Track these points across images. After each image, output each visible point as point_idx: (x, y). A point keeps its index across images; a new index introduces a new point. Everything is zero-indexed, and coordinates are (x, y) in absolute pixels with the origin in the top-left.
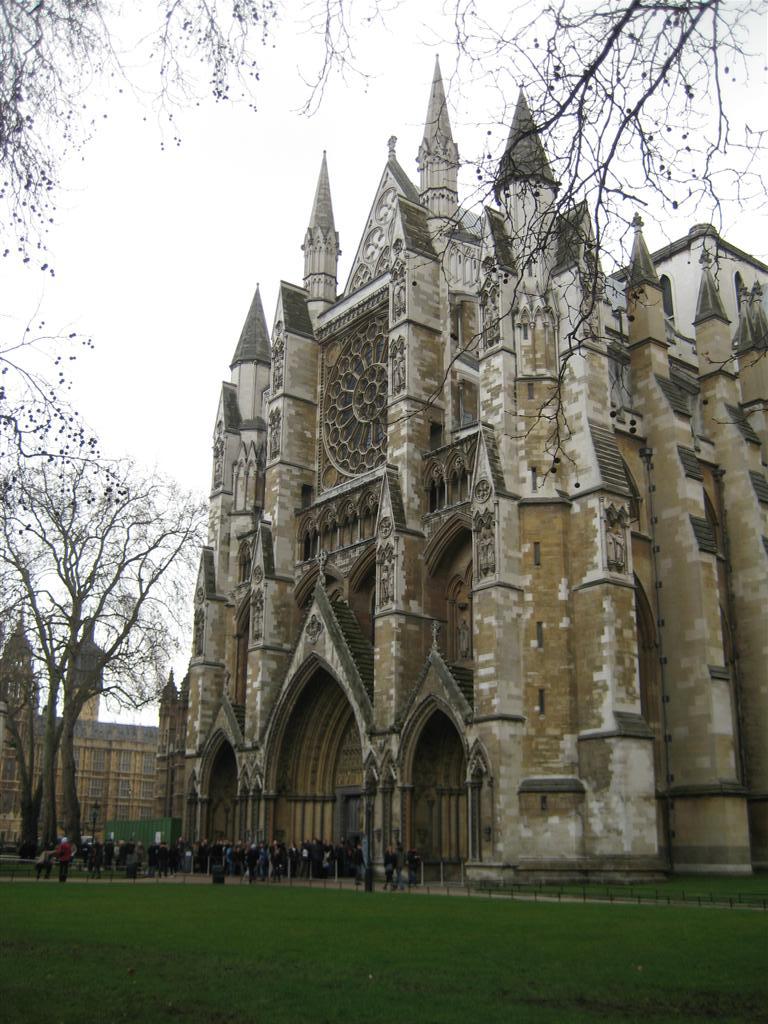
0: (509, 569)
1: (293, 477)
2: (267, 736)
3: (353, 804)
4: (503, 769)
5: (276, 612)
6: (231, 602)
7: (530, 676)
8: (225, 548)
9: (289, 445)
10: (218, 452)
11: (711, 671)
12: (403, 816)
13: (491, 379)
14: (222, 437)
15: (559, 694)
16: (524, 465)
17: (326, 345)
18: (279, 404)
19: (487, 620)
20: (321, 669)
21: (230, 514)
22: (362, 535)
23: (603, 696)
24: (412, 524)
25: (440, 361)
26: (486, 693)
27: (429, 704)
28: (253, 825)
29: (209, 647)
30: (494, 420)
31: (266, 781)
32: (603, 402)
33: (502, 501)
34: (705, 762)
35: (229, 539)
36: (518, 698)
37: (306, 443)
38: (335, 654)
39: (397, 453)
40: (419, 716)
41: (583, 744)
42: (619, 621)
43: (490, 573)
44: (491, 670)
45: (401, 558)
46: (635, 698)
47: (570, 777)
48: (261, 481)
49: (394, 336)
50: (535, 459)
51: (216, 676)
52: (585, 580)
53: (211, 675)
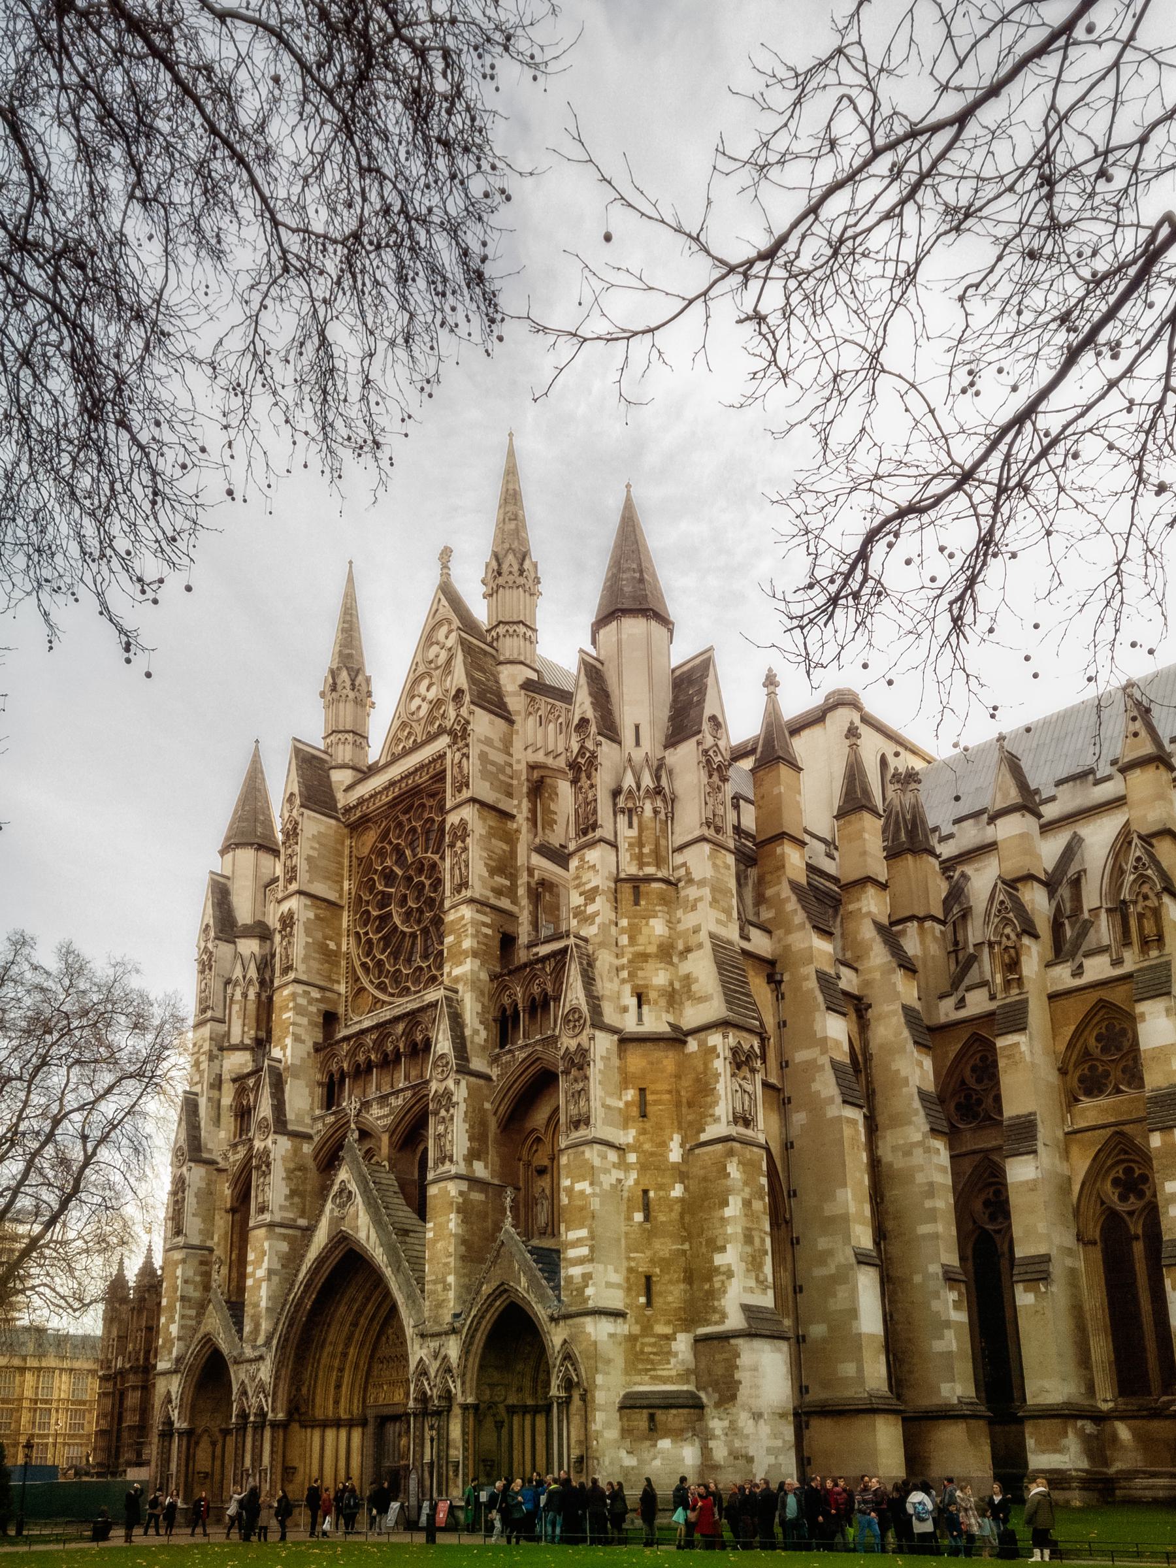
0: (608, 1122)
1: (311, 1001)
2: (275, 1342)
3: (392, 1429)
4: (599, 1379)
6: (222, 1164)
7: (634, 1259)
8: (215, 1094)
9: (306, 959)
10: (206, 965)
11: (856, 1254)
12: (465, 1441)
15: (670, 1282)
16: (627, 989)
17: (357, 825)
19: (578, 1187)
20: (351, 1251)
21: (221, 1049)
22: (407, 1078)
23: (727, 1283)
24: (478, 1063)
25: (513, 854)
26: (578, 1280)
27: (500, 1295)
28: (253, 1460)
29: (193, 1225)
30: (589, 931)
32: (728, 912)
33: (598, 1033)
34: (848, 1369)
35: (221, 1081)
36: (618, 1286)
37: (330, 957)
39: (457, 971)
40: (487, 1311)
41: (700, 1345)
42: (747, 1190)
43: (583, 1126)
44: (584, 1251)
45: (463, 1107)
46: (767, 1287)
47: (685, 1388)
48: (265, 1010)
49: (453, 819)
50: (641, 983)
51: (202, 1263)
52: (704, 1137)
53: (193, 1263)
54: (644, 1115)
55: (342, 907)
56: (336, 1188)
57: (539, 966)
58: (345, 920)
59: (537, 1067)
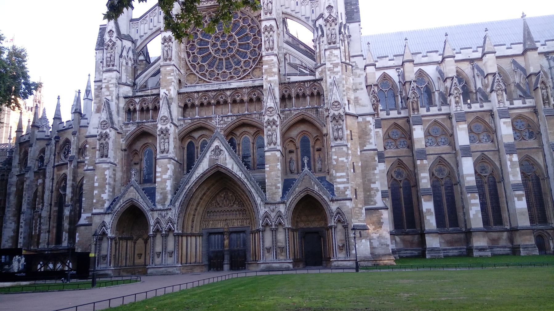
2: (177, 204)
5: (174, 141)
6: (120, 131)
8: (117, 101)
13: (333, 58)
14: (114, 39)
19: (340, 159)
21: (119, 84)
30: (337, 77)
31: (177, 226)
37: (180, 57)
39: (269, 79)
41: (367, 211)
43: (339, 139)
44: (345, 180)
51: (114, 170)
52: (365, 148)
53: (111, 170)
54: (352, 139)
56: (212, 148)
57: (302, 83)
59: (301, 117)
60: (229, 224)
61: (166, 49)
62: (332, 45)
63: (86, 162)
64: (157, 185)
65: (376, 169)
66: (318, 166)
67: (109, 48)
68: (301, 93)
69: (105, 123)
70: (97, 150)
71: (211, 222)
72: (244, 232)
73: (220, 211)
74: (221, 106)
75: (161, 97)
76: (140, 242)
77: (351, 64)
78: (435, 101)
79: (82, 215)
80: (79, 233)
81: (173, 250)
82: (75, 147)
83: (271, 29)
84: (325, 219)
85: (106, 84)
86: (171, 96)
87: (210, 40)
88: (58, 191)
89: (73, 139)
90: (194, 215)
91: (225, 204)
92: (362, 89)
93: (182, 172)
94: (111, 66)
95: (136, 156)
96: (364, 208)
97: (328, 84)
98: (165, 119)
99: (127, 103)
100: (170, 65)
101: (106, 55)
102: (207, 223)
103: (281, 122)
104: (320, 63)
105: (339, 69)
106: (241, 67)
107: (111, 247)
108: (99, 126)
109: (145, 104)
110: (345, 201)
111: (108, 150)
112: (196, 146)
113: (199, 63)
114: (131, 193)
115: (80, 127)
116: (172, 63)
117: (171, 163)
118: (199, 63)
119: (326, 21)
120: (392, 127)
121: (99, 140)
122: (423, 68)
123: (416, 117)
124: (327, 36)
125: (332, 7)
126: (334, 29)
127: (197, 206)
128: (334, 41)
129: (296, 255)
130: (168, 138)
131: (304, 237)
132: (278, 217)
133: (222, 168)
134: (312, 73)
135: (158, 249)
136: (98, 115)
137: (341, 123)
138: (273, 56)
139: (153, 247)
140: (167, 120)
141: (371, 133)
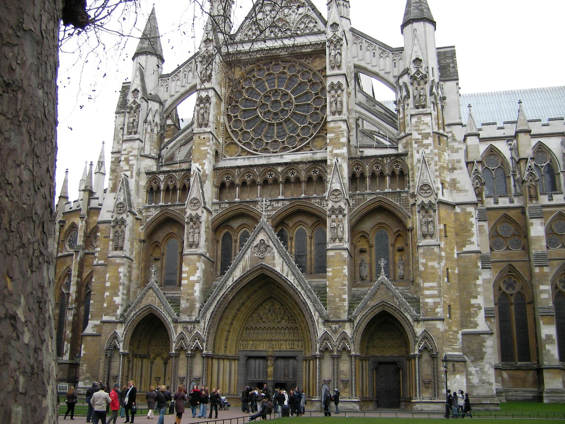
2: (208, 315)
5: (206, 232)
6: (139, 216)
13: (421, 128)
14: (138, 101)
16: (439, 180)
18: (211, 94)
19: (430, 264)
21: (141, 156)
31: (207, 345)
38: (286, 268)
39: (336, 151)
41: (464, 336)
43: (428, 237)
44: (436, 292)
51: (130, 267)
52: (465, 249)
55: (221, 100)
58: (223, 106)
60: (274, 346)
61: (202, 111)
62: (421, 110)
63: (97, 254)
64: (182, 288)
65: (478, 279)
66: (400, 271)
67: (132, 111)
68: (377, 171)
69: (122, 206)
70: (111, 240)
71: (251, 342)
72: (294, 358)
73: (262, 328)
74: (270, 186)
75: (192, 173)
76: (159, 362)
77: (446, 134)
78: (560, 185)
79: (90, 322)
80: (85, 345)
81: (201, 376)
82: (83, 235)
83: (339, 87)
84: (406, 344)
85: (126, 156)
86: (204, 172)
87: (258, 100)
88: (61, 288)
89: (81, 224)
90: (229, 332)
91: (270, 318)
92: (461, 168)
93: (214, 273)
94: (133, 133)
95: (157, 250)
96: (460, 332)
97: (415, 160)
98: (196, 202)
99: (150, 181)
100: (205, 133)
101: (128, 119)
102: (245, 343)
103: (350, 210)
104: (405, 132)
105: (430, 141)
106: (298, 135)
107: (123, 365)
108: (114, 210)
109: (172, 181)
110: (435, 322)
111: (123, 241)
112: (234, 238)
113: (242, 129)
114: (150, 298)
115: (91, 209)
116: (208, 130)
117: (201, 260)
118: (242, 129)
119: (413, 78)
120: (501, 221)
121: (114, 227)
122: (543, 140)
123: (534, 207)
124: (415, 97)
125: (421, 60)
126: (422, 89)
127: (233, 320)
128: (423, 104)
129: (364, 392)
130: (198, 228)
131: (376, 369)
132: (342, 339)
133: (267, 270)
134: (394, 145)
135: (182, 372)
136: (114, 194)
137: (432, 213)
138: (341, 122)
139: (175, 370)
140: (198, 204)
141: (472, 229)
